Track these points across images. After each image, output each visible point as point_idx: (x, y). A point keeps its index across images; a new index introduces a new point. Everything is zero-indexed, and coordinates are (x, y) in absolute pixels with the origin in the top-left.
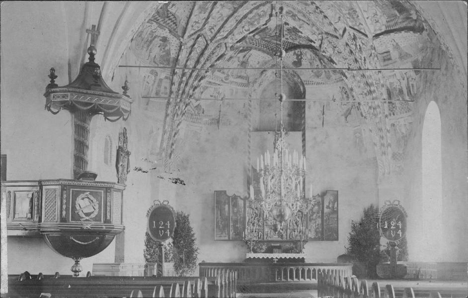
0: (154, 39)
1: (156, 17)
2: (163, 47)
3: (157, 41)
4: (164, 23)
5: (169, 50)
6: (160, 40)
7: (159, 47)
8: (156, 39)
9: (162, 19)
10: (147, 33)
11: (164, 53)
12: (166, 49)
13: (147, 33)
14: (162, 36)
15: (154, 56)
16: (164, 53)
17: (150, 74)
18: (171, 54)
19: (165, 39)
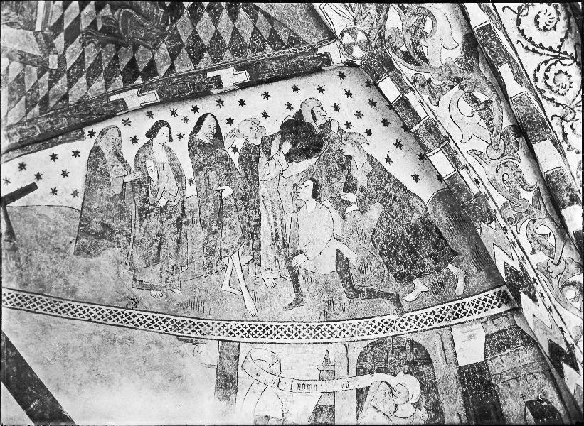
0: (253, 178)
1: (124, 63)
2: (340, 185)
3: (281, 175)
4: (196, 60)
5: (379, 173)
6: (289, 157)
7: (315, 195)
8: (267, 170)
9: (163, 50)
10: (179, 177)
11: (375, 211)
12: (361, 180)
13: (179, 177)
14: (272, 127)
15: (329, 265)
16: (375, 211)
17: (365, 381)
18: (411, 186)
19: (303, 136)
